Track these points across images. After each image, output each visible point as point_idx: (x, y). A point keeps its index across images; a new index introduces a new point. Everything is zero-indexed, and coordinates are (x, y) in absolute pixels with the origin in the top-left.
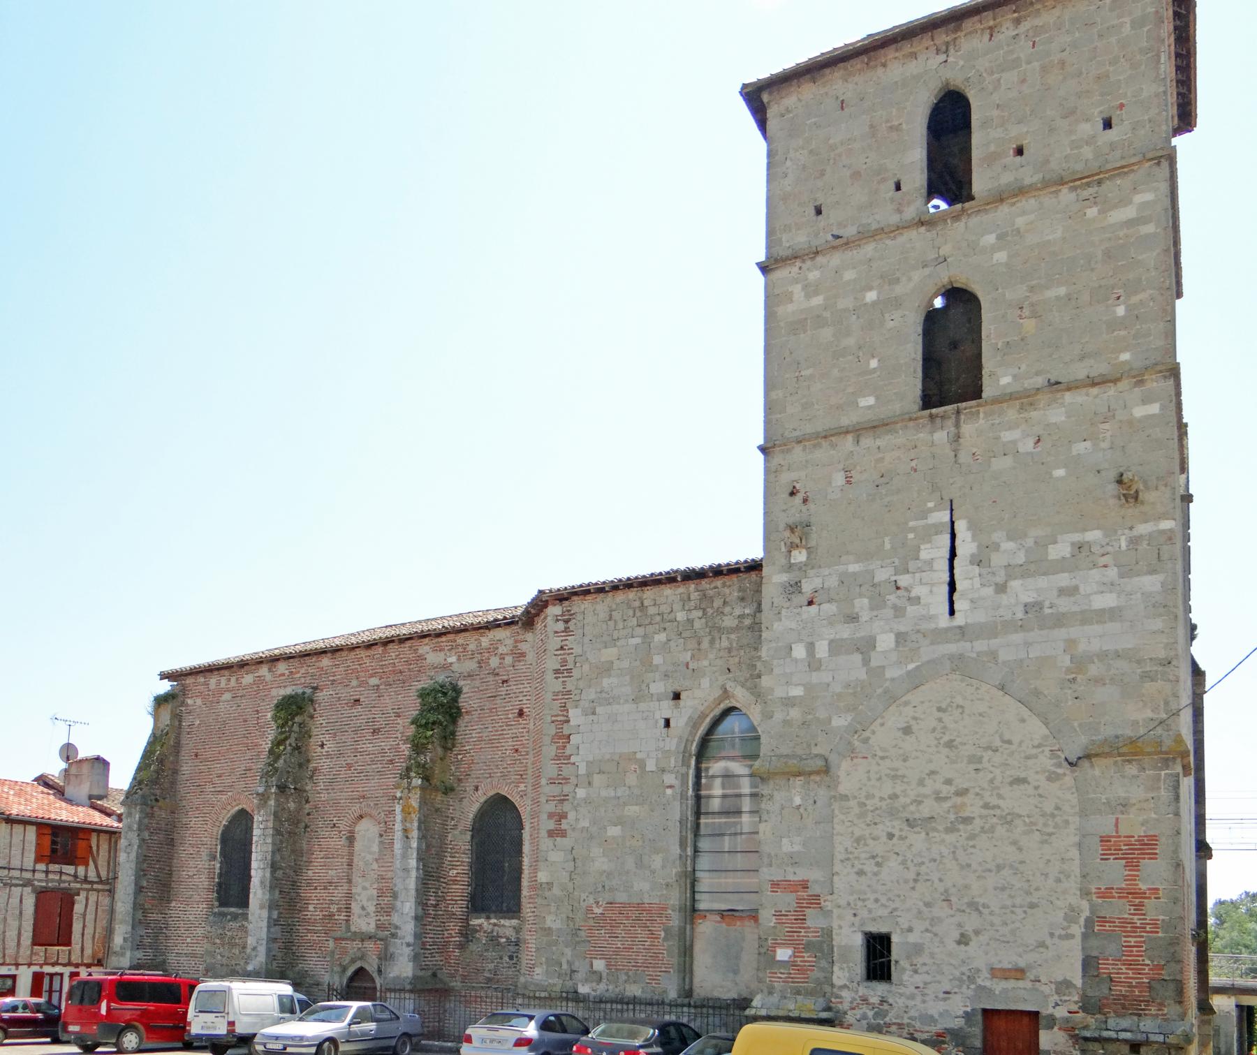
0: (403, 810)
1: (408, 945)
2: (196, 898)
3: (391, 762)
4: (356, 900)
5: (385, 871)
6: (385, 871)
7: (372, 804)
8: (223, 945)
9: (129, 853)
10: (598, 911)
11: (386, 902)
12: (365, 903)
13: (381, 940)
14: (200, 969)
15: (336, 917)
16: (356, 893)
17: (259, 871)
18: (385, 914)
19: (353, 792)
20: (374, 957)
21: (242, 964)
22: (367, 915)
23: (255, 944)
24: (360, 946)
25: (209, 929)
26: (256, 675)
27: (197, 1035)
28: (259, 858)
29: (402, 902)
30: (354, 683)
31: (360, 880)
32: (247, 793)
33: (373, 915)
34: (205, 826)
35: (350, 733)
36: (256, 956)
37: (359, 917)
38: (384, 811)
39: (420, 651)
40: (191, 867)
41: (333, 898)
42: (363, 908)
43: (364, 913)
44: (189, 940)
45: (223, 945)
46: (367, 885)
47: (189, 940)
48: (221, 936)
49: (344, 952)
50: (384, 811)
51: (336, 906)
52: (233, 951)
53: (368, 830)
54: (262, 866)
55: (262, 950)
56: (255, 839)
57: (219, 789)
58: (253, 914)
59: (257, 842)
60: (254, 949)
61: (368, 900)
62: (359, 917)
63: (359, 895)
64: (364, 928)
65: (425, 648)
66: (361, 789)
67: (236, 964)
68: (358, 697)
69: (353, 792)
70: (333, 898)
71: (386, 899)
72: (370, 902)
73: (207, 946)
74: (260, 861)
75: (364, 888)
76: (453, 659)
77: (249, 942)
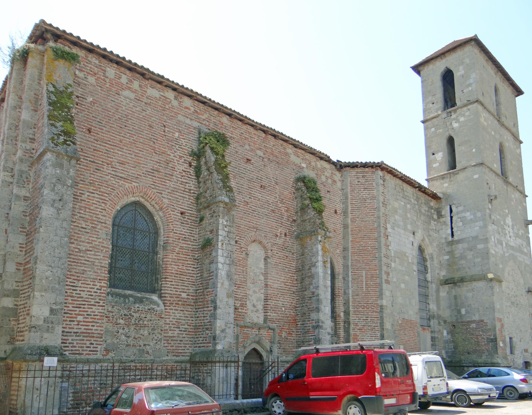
0: (322, 249)
1: (329, 334)
2: (91, 274)
3: (273, 211)
4: (249, 300)
5: (273, 283)
6: (273, 283)
7: (263, 235)
8: (128, 326)
9: (58, 210)
10: (400, 322)
11: (273, 304)
12: (255, 302)
13: (271, 329)
14: (98, 349)
15: (240, 310)
16: (249, 294)
17: (225, 265)
18: (273, 312)
19: (250, 222)
20: (267, 341)
21: (152, 344)
22: (257, 311)
23: (223, 327)
24: (257, 333)
25: (110, 309)
26: (162, 94)
27: (433, 395)
28: (225, 255)
29: (324, 306)
30: (247, 147)
31: (251, 285)
32: (156, 191)
33: (261, 311)
34: (103, 205)
35: (245, 180)
36: (225, 337)
37: (252, 312)
38: (270, 242)
39: (288, 151)
40: (83, 242)
41: (237, 296)
42: (254, 306)
43: (255, 309)
44: (80, 318)
45: (128, 326)
46: (257, 289)
47: (80, 318)
48: (128, 317)
49: (247, 337)
50: (270, 242)
51: (240, 302)
52: (142, 332)
53: (256, 252)
54: (228, 262)
55: (230, 332)
56: (220, 238)
57: (123, 176)
58: (221, 301)
59: (222, 241)
60: (223, 331)
61: (257, 301)
62: (252, 312)
63: (251, 296)
64: (256, 320)
65: (290, 150)
66: (255, 222)
67: (145, 345)
68: (250, 158)
69: (250, 222)
70: (237, 296)
71: (273, 302)
72: (259, 303)
73: (107, 325)
74: (226, 257)
75: (254, 292)
76: (304, 165)
77: (218, 325)
